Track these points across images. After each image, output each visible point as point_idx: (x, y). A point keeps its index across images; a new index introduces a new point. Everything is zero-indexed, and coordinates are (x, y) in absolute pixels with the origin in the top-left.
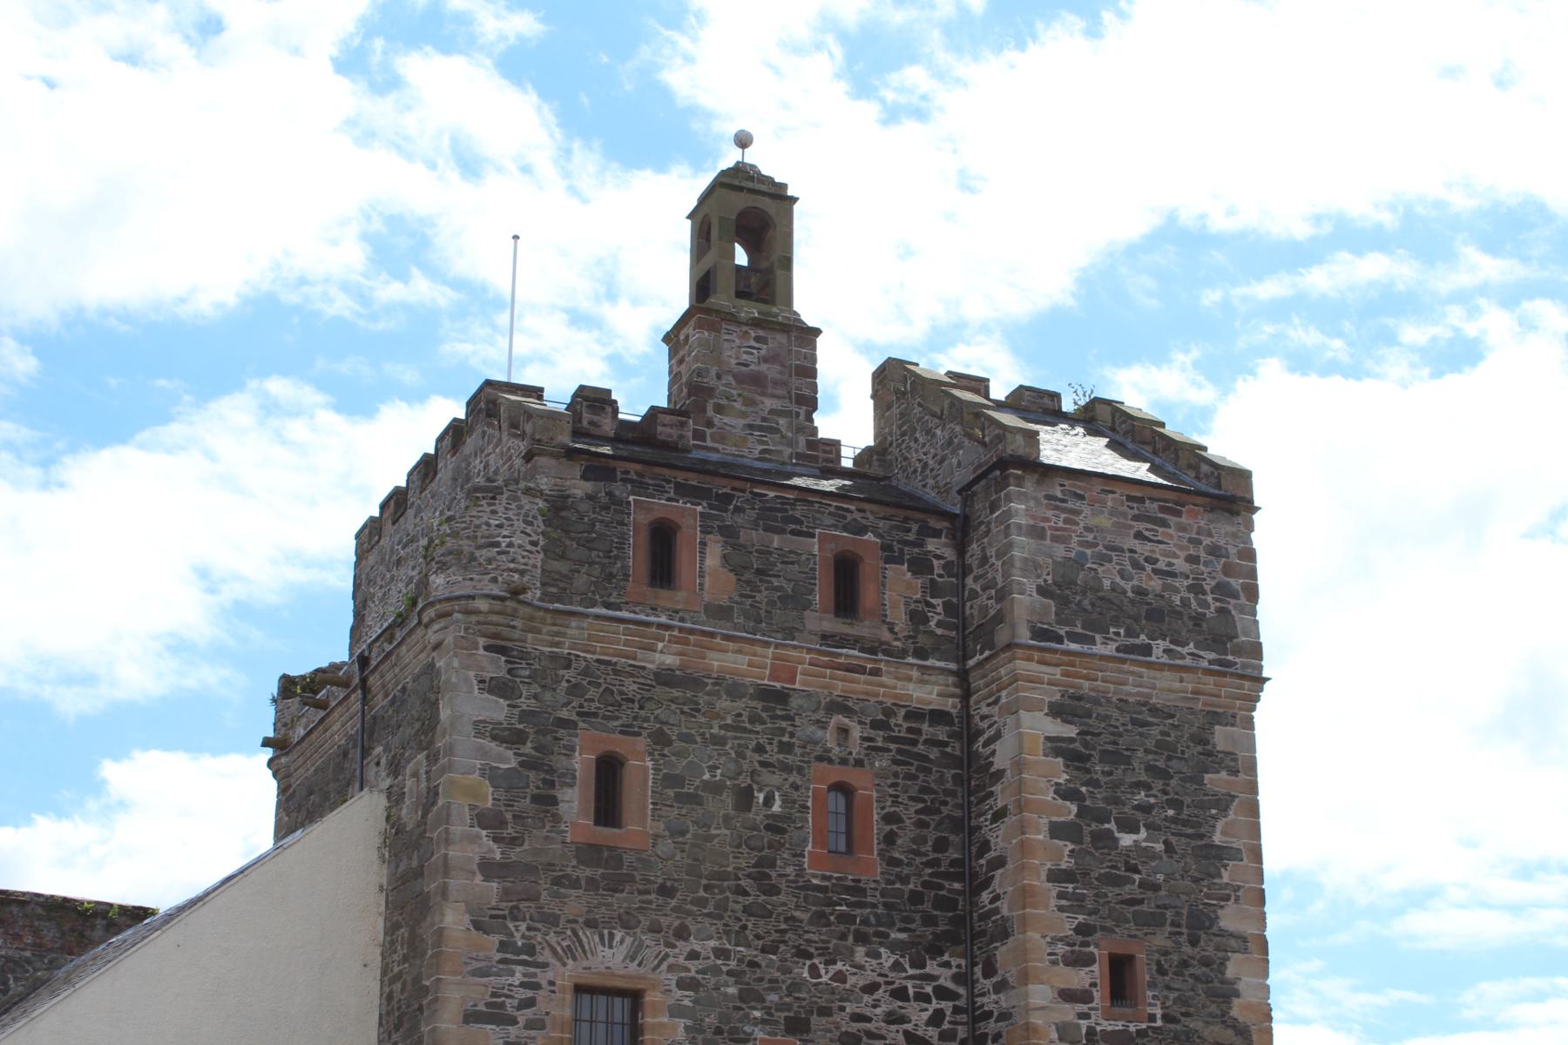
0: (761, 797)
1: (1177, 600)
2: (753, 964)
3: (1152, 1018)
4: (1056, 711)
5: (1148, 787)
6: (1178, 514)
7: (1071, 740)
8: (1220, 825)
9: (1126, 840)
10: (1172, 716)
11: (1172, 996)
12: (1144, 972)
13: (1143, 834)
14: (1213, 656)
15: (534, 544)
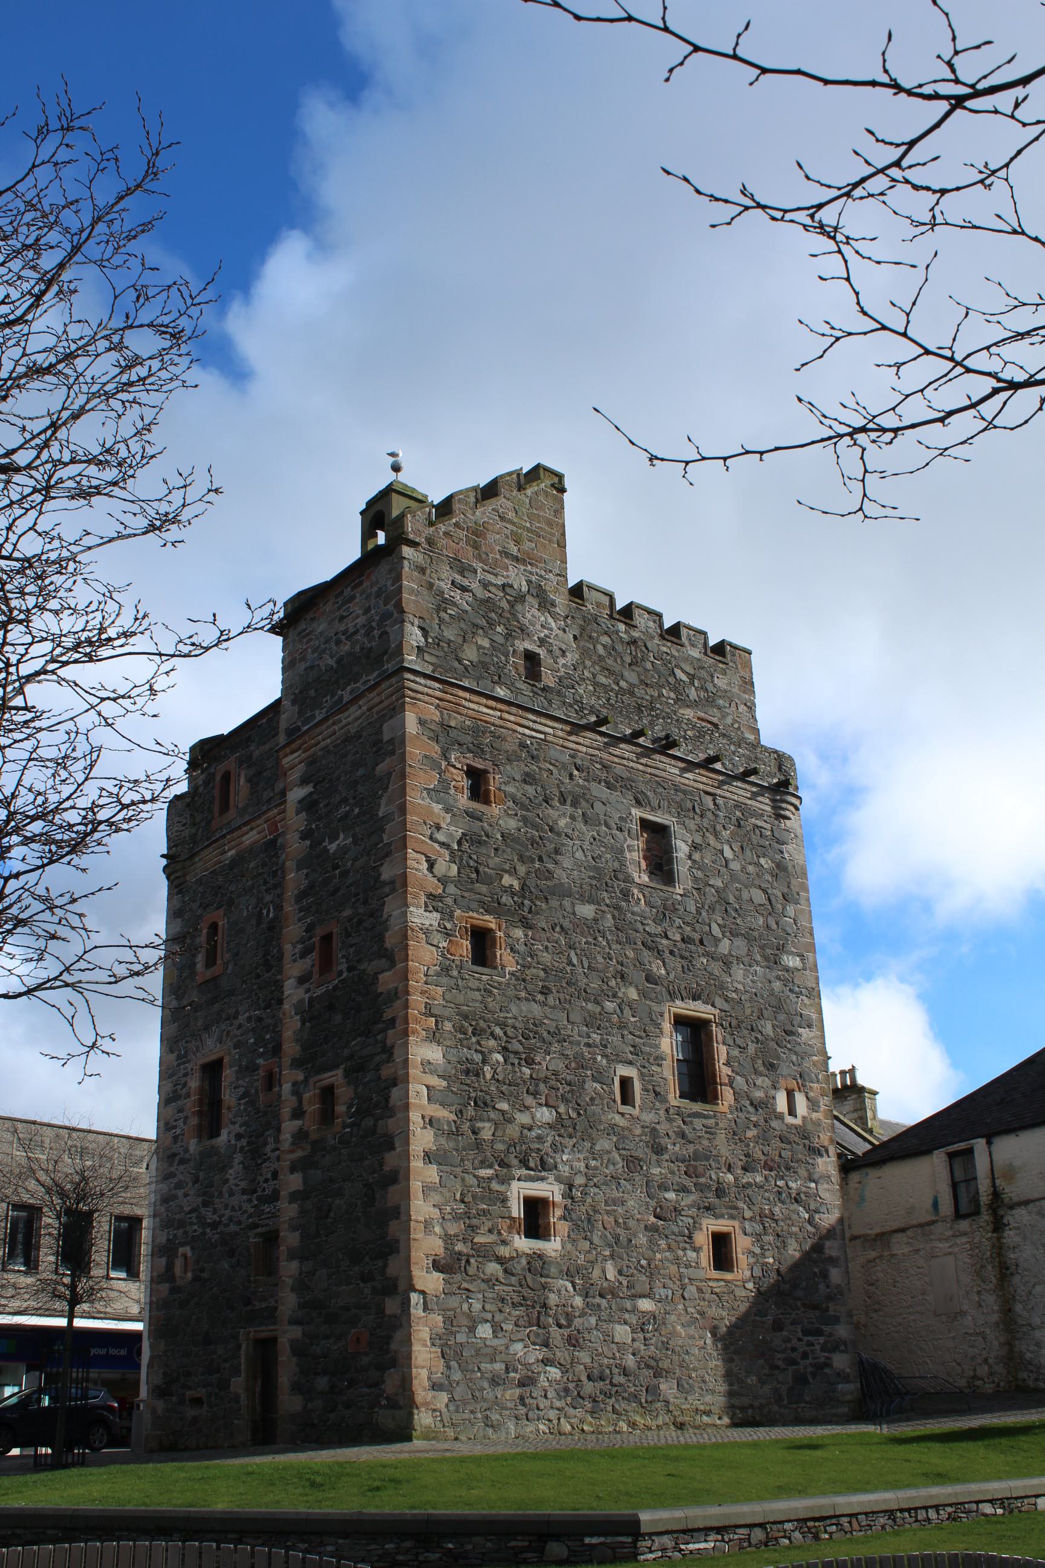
0: (265, 912)
1: (357, 648)
2: (260, 1019)
3: (340, 973)
4: (304, 781)
5: (345, 800)
6: (361, 583)
7: (311, 794)
8: (383, 802)
9: (333, 847)
10: (360, 737)
11: (352, 950)
12: (336, 943)
13: (342, 836)
14: (376, 673)
15: (184, 825)
